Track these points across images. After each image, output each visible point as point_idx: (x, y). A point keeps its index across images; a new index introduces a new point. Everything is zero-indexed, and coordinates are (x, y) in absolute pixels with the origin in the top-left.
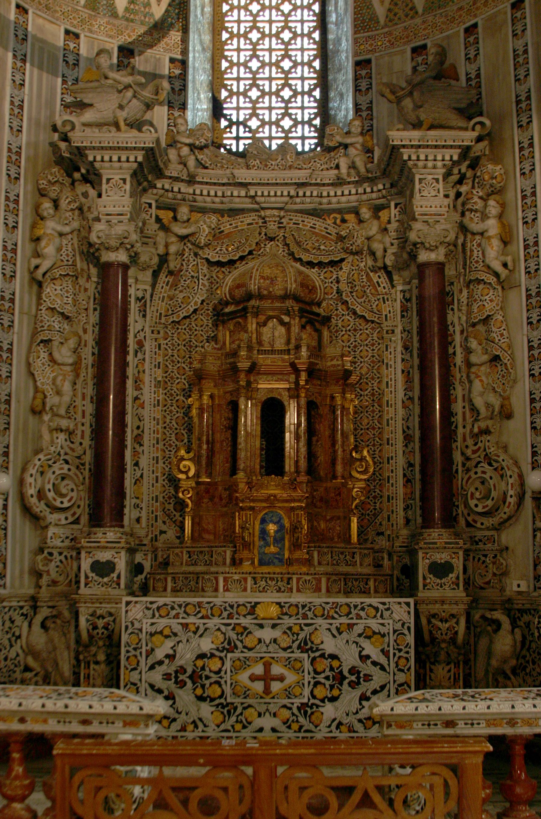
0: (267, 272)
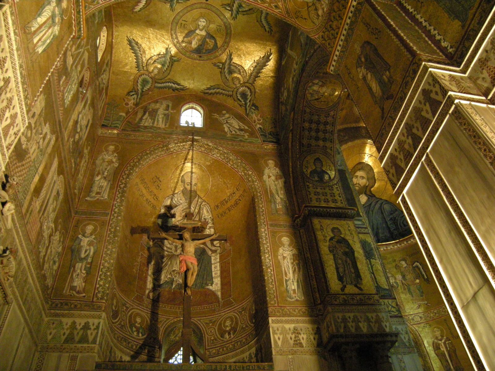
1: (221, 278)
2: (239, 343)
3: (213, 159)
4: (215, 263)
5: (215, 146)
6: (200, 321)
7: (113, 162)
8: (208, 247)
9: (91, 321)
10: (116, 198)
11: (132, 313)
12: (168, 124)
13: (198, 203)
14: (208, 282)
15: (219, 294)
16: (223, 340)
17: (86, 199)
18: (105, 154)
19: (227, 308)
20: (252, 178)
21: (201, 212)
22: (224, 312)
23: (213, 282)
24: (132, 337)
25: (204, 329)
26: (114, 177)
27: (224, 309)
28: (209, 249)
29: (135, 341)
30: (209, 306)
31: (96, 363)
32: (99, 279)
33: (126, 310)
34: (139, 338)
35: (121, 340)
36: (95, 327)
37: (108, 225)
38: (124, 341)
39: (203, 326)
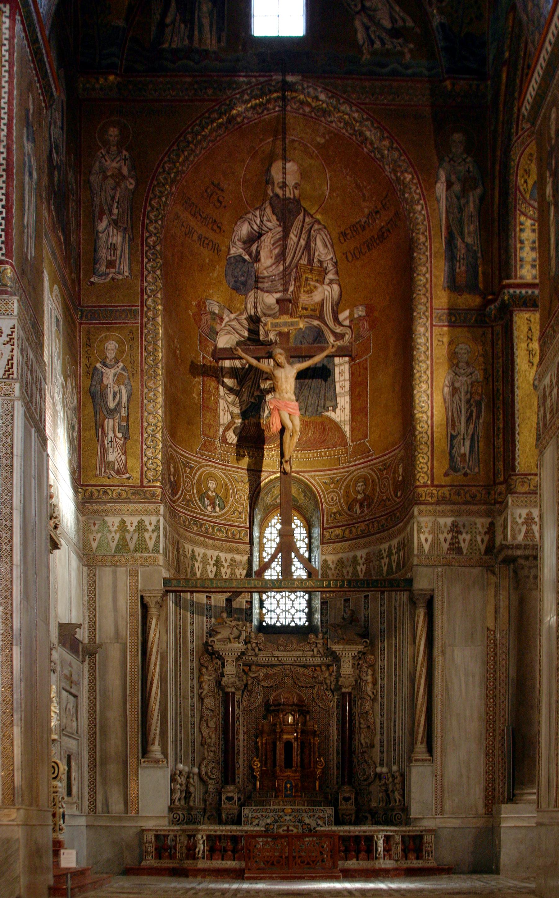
0: (286, 695)
1: (351, 399)
2: (376, 525)
3: (330, 132)
4: (341, 364)
5: (333, 101)
6: (315, 480)
7: (124, 177)
8: (328, 326)
9: (146, 519)
10: (146, 273)
11: (200, 476)
12: (224, 36)
13: (305, 225)
14: (328, 403)
15: (347, 429)
16: (350, 516)
17: (92, 280)
18: (103, 156)
19: (359, 459)
20: (410, 193)
21: (312, 245)
22: (355, 465)
23: (337, 404)
24: (204, 515)
25: (321, 493)
26: (131, 217)
27: (355, 460)
28: (330, 329)
29: (210, 522)
30: (330, 452)
31: (165, 579)
32: (145, 447)
33: (190, 473)
34: (216, 514)
35: (190, 524)
36: (153, 527)
37: (142, 338)
38: (194, 524)
39: (319, 489)
